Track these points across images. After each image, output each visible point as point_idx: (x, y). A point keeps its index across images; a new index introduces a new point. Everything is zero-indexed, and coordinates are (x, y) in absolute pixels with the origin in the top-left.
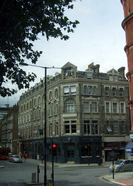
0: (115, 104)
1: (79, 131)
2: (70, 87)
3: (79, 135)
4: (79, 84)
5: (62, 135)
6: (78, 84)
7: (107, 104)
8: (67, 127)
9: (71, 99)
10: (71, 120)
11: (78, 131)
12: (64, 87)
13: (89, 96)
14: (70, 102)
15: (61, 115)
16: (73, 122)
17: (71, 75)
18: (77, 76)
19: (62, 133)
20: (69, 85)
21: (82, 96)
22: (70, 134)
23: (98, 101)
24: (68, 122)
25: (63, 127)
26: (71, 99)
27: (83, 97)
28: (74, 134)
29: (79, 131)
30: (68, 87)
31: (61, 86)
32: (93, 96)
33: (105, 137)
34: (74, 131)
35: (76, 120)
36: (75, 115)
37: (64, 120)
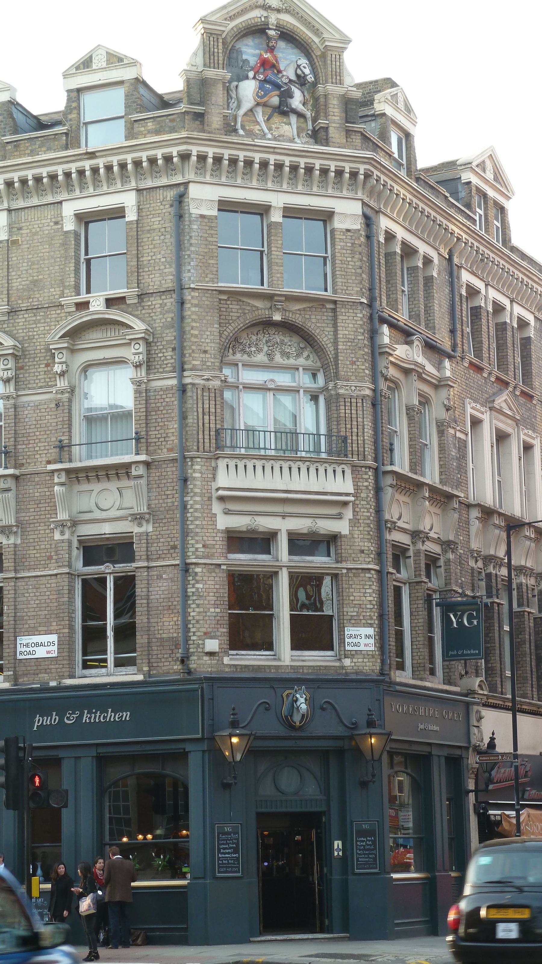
0: (501, 437)
1: (370, 631)
2: (276, 217)
3: (371, 667)
4: (364, 203)
5: (202, 665)
6: (356, 208)
7: (476, 423)
8: (248, 595)
9: (287, 327)
10: (301, 525)
11: (361, 638)
12: (225, 206)
13: (405, 335)
14: (261, 358)
15: (197, 471)
16: (300, 543)
17: (283, 110)
18: (348, 132)
19: (211, 645)
20: (278, 200)
21: (383, 321)
22: (285, 655)
23: (444, 393)
24: (263, 542)
25: (209, 596)
26: (287, 327)
27: (385, 329)
28: (314, 658)
29: (370, 631)
30: (262, 210)
31: (194, 191)
32: (430, 347)
33: (485, 705)
34: (313, 631)
35: (342, 527)
36: (341, 484)
37: (224, 522)
